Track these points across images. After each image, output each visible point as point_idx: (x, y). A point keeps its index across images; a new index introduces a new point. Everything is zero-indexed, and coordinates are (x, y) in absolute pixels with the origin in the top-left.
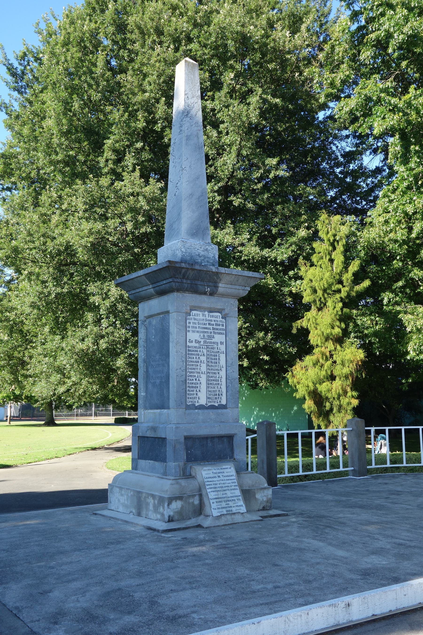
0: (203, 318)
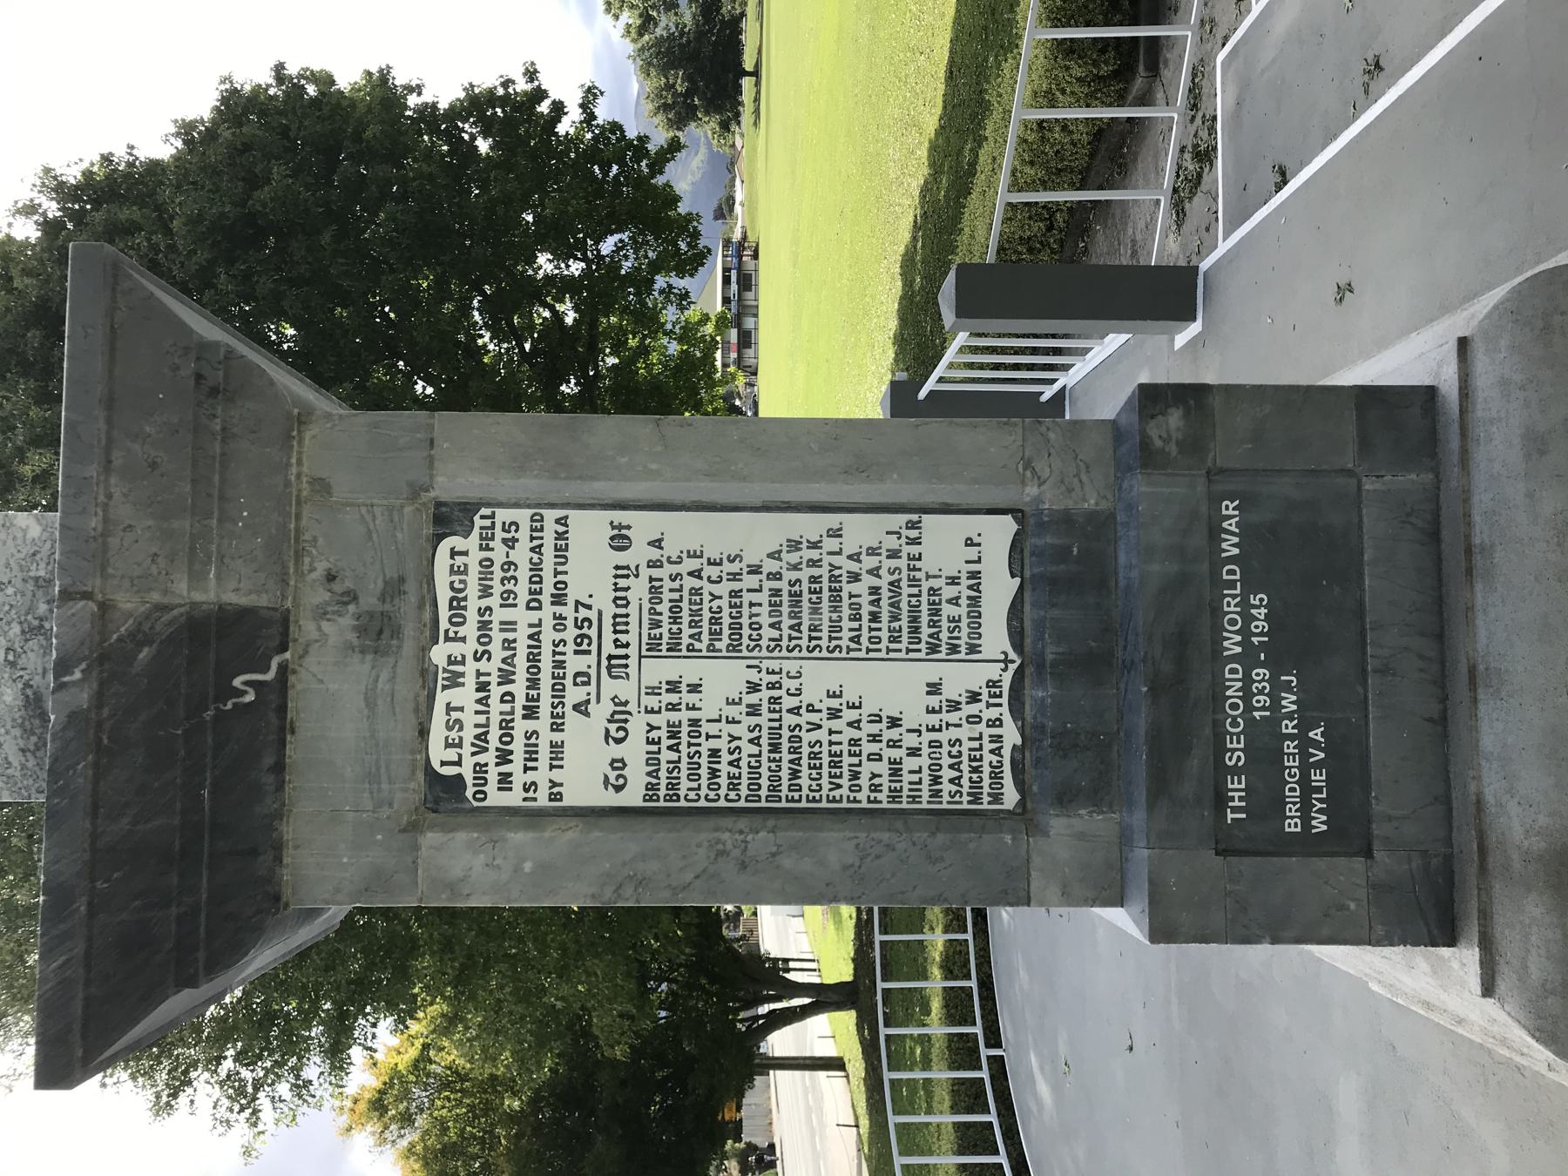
0: (470, 681)
